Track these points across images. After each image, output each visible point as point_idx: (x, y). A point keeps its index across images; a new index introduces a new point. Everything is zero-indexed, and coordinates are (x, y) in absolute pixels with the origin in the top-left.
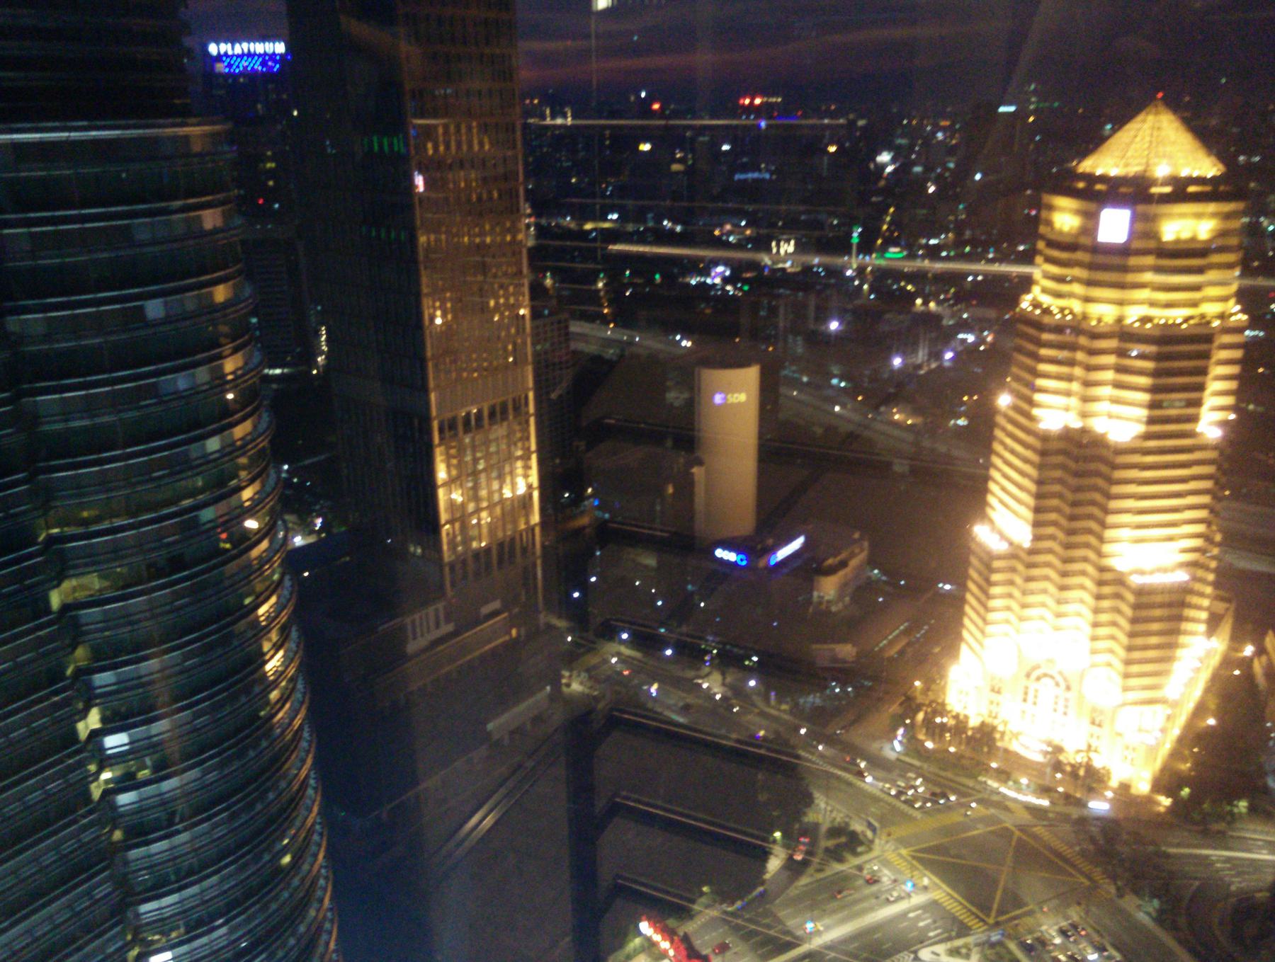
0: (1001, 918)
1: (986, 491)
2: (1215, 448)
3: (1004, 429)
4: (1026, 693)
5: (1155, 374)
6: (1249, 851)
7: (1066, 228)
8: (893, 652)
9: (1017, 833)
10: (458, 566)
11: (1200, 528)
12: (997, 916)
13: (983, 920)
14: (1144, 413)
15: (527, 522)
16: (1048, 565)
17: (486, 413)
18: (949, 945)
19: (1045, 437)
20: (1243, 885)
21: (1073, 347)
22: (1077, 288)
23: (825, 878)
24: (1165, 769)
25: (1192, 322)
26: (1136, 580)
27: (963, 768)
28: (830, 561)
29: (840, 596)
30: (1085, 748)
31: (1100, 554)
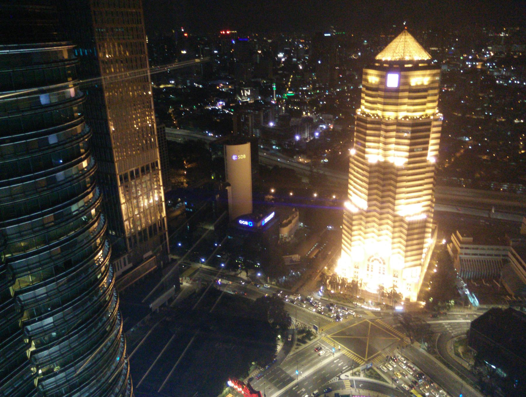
0: (369, 358)
1: (347, 188)
2: (433, 165)
3: (353, 163)
4: (368, 267)
5: (411, 138)
6: (456, 319)
7: (374, 82)
8: (313, 256)
9: (370, 323)
10: (132, 238)
11: (429, 197)
12: (367, 358)
13: (362, 360)
14: (407, 154)
15: (161, 216)
16: (374, 216)
17: (140, 170)
18: (351, 372)
19: (371, 166)
20: (456, 333)
21: (379, 130)
22: (379, 106)
23: (299, 351)
24: (421, 291)
25: (423, 117)
26: (407, 219)
27: (346, 299)
28: (285, 221)
29: (290, 236)
30: (392, 286)
31: (394, 210)
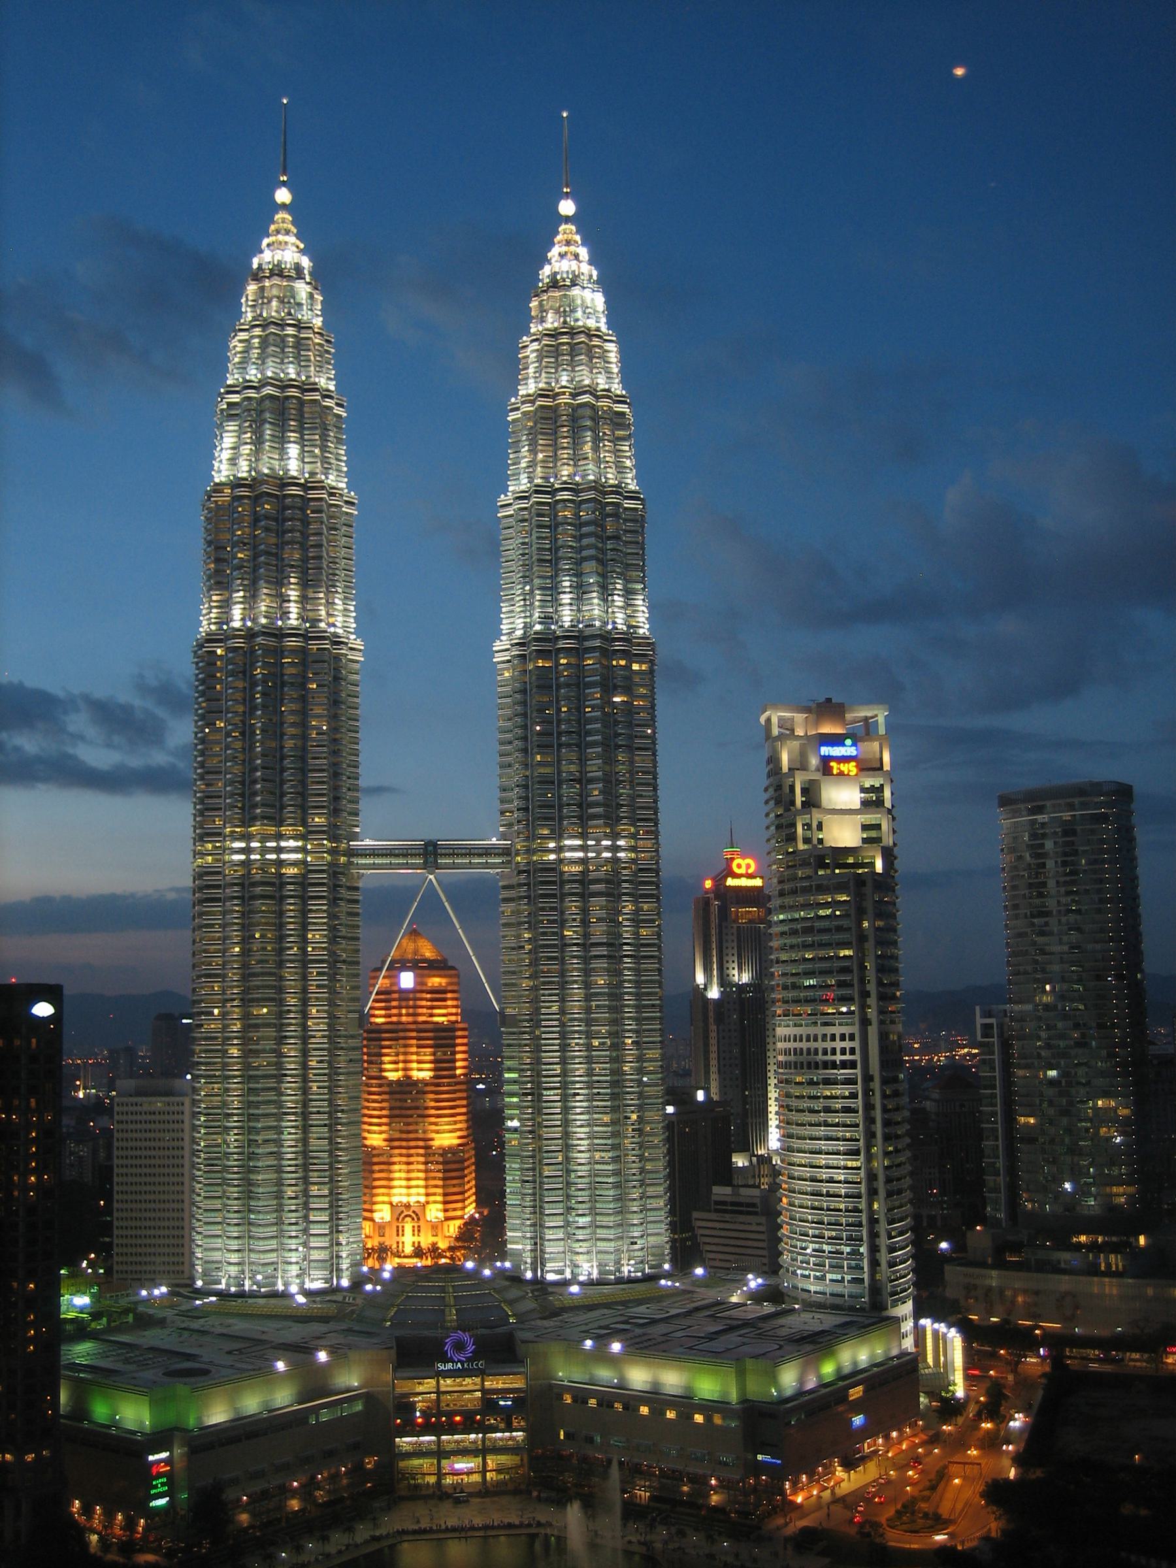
4: (398, 1231)
